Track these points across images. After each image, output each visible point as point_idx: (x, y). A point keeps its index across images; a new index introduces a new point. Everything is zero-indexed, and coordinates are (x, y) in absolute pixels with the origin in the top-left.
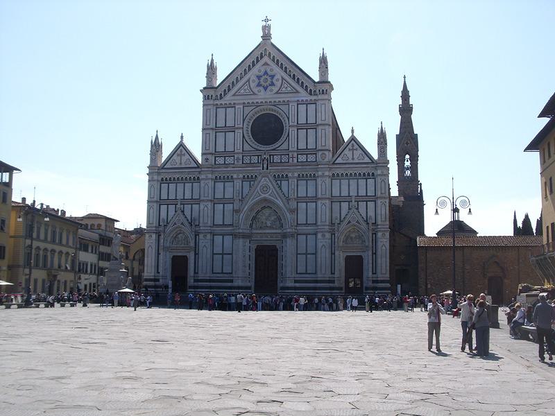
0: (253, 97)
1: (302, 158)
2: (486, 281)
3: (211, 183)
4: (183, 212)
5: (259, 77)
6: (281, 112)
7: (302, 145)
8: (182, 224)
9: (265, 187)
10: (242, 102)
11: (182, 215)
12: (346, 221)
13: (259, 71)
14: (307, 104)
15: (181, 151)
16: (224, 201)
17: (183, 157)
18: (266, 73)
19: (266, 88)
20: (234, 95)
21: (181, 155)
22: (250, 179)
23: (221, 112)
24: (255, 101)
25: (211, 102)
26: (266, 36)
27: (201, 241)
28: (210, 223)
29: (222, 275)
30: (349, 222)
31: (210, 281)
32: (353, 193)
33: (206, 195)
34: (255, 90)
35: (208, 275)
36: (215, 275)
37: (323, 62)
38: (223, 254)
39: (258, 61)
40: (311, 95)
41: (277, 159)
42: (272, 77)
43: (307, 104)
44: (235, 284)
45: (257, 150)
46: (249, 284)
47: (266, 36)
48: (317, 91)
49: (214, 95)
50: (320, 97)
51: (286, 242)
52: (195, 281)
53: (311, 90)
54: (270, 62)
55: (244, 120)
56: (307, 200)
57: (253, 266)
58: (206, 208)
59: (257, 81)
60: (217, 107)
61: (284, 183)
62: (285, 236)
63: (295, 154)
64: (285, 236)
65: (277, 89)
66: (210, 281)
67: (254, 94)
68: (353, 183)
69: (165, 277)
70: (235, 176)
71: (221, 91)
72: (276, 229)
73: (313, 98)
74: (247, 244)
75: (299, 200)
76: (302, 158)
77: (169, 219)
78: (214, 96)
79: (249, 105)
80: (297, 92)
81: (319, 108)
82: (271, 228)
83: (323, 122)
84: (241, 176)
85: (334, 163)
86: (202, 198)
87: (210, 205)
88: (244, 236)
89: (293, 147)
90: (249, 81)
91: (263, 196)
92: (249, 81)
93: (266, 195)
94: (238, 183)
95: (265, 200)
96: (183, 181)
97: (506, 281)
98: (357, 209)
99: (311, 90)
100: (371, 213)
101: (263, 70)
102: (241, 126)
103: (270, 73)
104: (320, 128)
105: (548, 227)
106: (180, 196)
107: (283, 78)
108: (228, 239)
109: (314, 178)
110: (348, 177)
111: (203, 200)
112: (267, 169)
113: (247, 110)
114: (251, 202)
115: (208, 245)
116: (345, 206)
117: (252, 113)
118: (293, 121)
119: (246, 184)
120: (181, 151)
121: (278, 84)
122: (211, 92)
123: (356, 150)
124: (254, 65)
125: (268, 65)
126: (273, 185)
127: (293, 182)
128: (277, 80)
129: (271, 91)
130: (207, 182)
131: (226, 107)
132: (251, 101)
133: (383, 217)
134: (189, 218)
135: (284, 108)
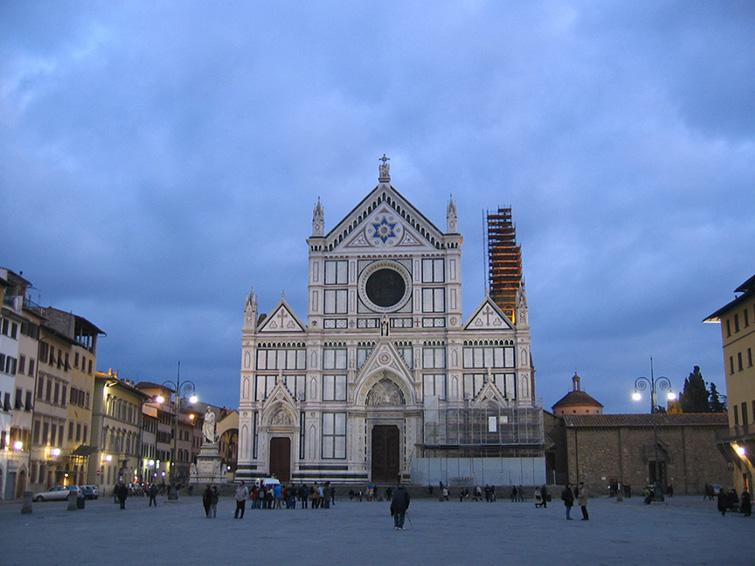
0: (367, 249)
1: (428, 323)
2: (647, 466)
3: (320, 351)
4: (285, 384)
5: (376, 226)
6: (401, 268)
7: (428, 308)
8: (284, 399)
9: (385, 359)
10: (357, 255)
11: (284, 389)
12: (482, 396)
13: (377, 219)
14: (433, 259)
15: (283, 311)
16: (335, 372)
17: (285, 319)
18: (384, 221)
19: (384, 240)
20: (347, 246)
21: (282, 316)
22: (368, 347)
23: (331, 266)
24: (372, 255)
25: (320, 254)
26: (384, 178)
27: (307, 421)
28: (319, 399)
29: (332, 461)
30: (485, 398)
31: (320, 468)
32: (489, 365)
33: (314, 364)
34: (372, 242)
35: (317, 462)
36: (325, 461)
37: (452, 208)
38: (334, 436)
39: (375, 207)
40: (437, 247)
41: (398, 324)
42: (392, 226)
43: (433, 259)
44: (349, 472)
45: (375, 312)
46: (365, 472)
47: (384, 178)
48: (446, 245)
49: (322, 246)
50: (449, 252)
51: (409, 421)
52: (301, 468)
53: (438, 243)
54: (388, 208)
55: (358, 277)
56: (432, 371)
57: (369, 449)
58: (313, 380)
59: (374, 231)
60: (326, 260)
61: (407, 352)
62: (408, 414)
63: (420, 320)
64: (408, 414)
65: (398, 241)
66: (320, 468)
67: (371, 246)
68: (488, 352)
69: (263, 465)
70: (348, 343)
71: (330, 241)
72: (397, 406)
73: (441, 252)
74: (364, 424)
75: (426, 372)
76: (428, 323)
77: (268, 392)
78: (323, 248)
79: (364, 259)
80: (422, 245)
81: (448, 264)
82: (391, 404)
83: (453, 281)
84: (356, 343)
85: (465, 329)
86: (309, 369)
87: (319, 377)
88: (358, 414)
89: (417, 310)
90: (364, 229)
91: (383, 366)
92: (364, 229)
93: (387, 367)
94: (352, 352)
95: (385, 372)
96: (285, 346)
97: (670, 466)
98: (494, 382)
99: (438, 243)
100: (510, 390)
101: (381, 219)
102: (356, 284)
103: (389, 221)
104: (449, 288)
105: (736, 407)
106: (281, 366)
107: (404, 229)
108: (340, 418)
109: (444, 346)
110: (484, 345)
111: (311, 372)
112: (387, 334)
113: (363, 264)
114: (367, 375)
115: (318, 425)
116: (479, 379)
117: (369, 269)
118: (417, 280)
119: (362, 353)
120: (283, 311)
121: (399, 235)
122: (320, 243)
123: (492, 313)
124: (370, 211)
125: (387, 212)
126: (395, 355)
127: (418, 351)
128: (398, 230)
129: (391, 242)
130: (315, 349)
131: (337, 260)
132: (366, 255)
133: (525, 392)
134: (293, 391)
135: (407, 263)
